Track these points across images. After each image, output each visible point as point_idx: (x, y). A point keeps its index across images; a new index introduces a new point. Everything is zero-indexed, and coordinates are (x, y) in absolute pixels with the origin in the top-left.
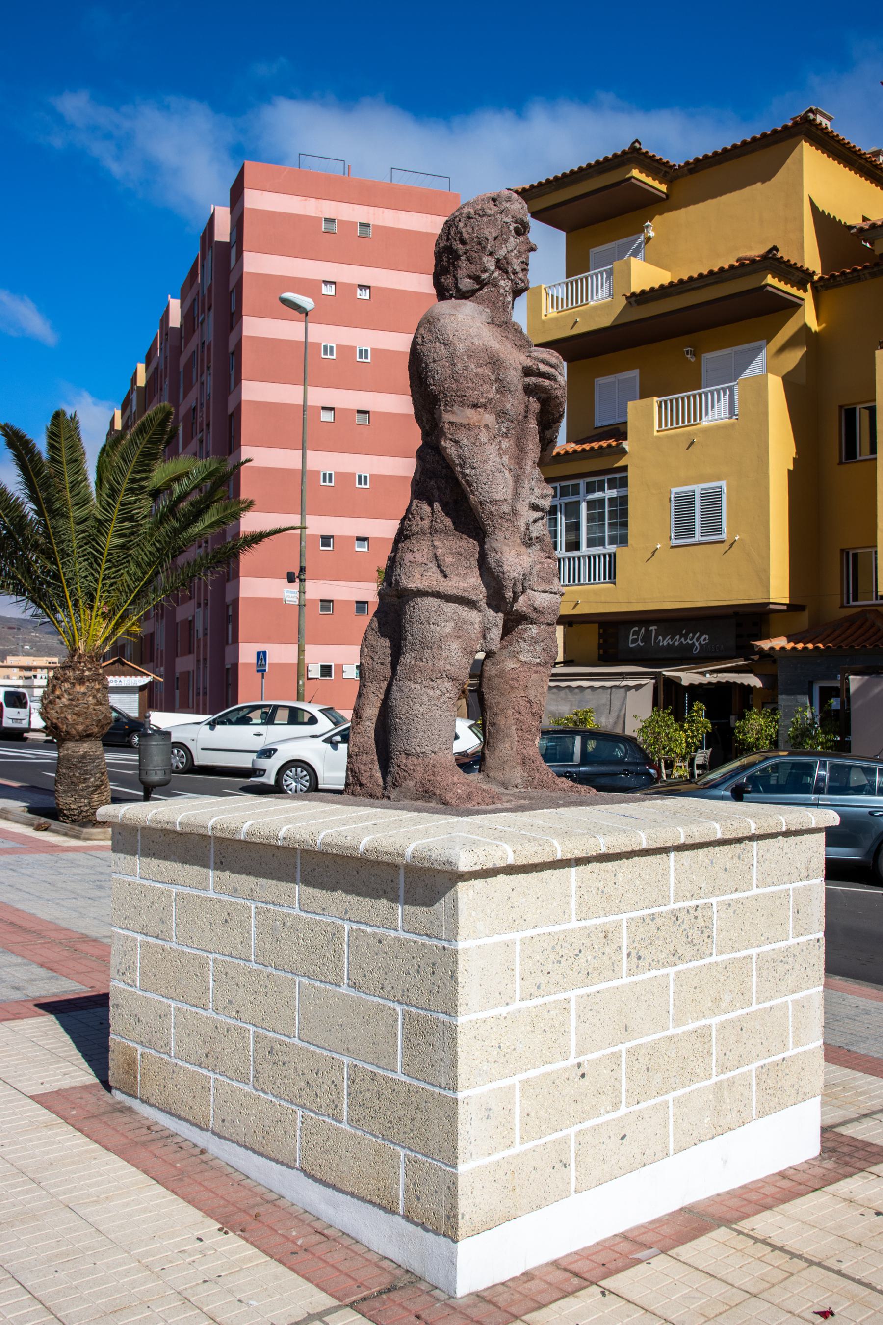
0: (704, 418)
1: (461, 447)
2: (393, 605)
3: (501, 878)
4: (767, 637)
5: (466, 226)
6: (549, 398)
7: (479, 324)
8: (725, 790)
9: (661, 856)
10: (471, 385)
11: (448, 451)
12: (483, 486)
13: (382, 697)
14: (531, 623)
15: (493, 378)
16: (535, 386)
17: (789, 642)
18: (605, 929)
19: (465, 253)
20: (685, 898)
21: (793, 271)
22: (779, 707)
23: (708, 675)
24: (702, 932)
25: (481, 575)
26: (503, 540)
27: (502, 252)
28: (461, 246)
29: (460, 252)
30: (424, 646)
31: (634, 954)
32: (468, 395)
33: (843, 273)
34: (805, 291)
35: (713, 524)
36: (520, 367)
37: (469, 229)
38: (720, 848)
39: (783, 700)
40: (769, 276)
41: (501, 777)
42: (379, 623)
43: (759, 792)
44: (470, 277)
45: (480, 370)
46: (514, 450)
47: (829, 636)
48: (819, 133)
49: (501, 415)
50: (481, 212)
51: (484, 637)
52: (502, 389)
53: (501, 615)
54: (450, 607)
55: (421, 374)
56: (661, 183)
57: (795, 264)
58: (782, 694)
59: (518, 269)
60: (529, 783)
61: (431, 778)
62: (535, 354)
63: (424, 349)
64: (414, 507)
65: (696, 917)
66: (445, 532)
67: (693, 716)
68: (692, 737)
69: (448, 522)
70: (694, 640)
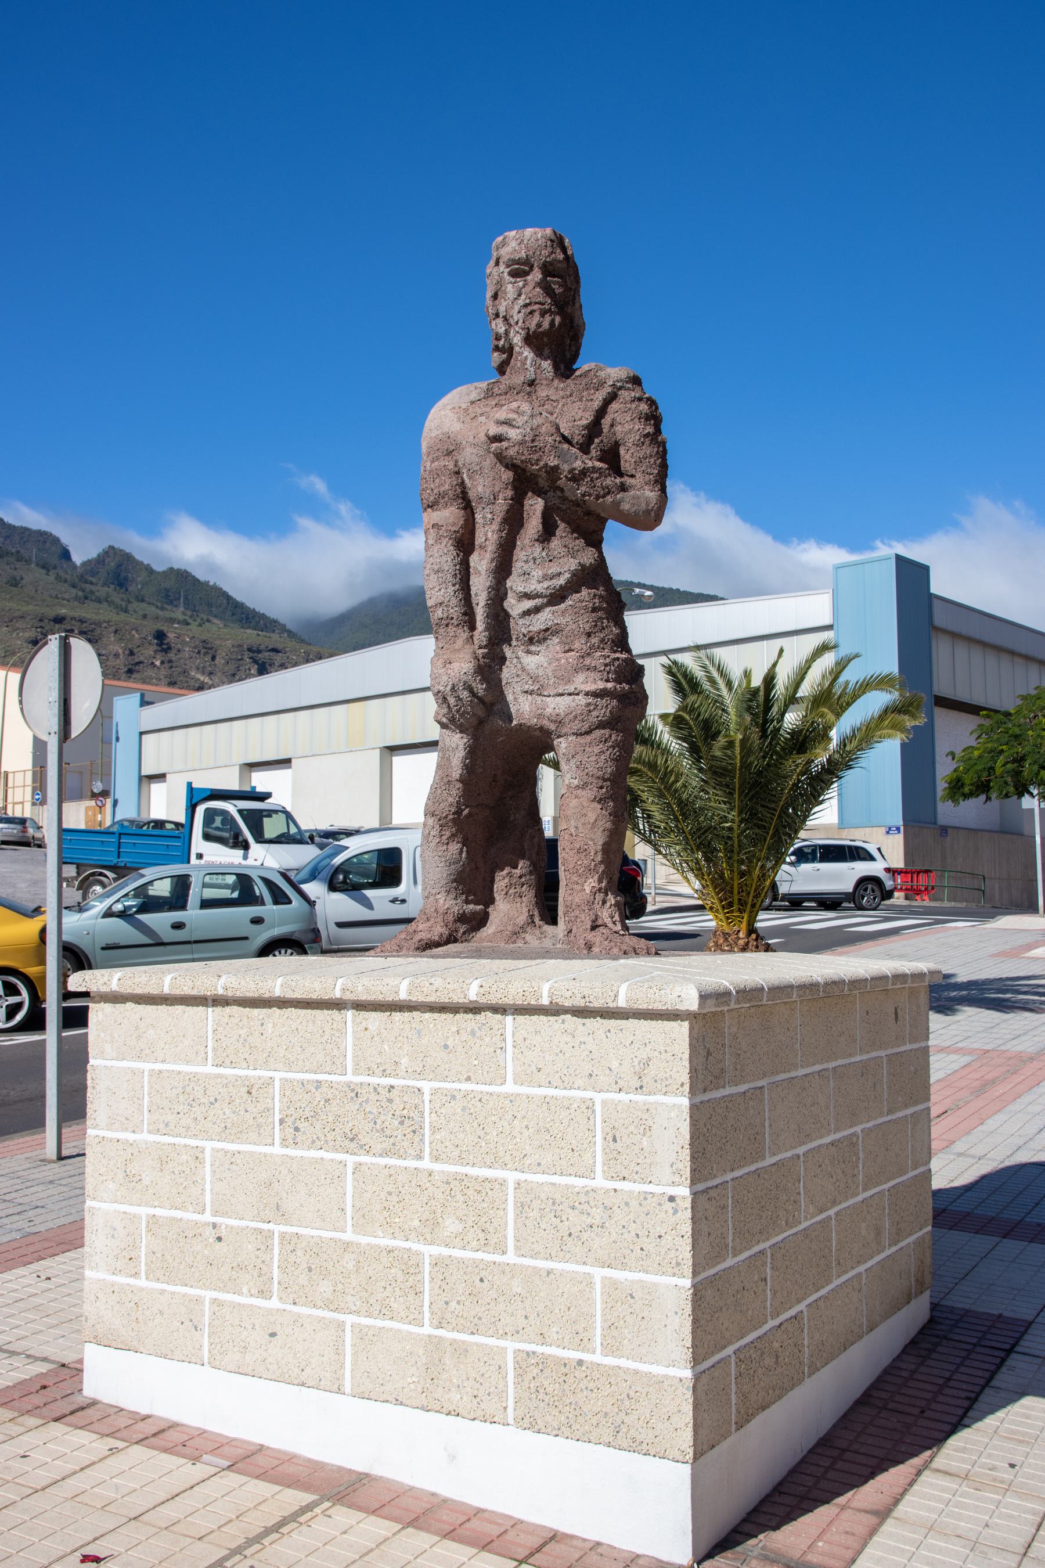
3: (130, 1005)
9: (330, 1012)
18: (247, 1083)
20: (370, 1072)
24: (402, 1123)
31: (289, 1121)
38: (436, 1015)
65: (390, 1101)
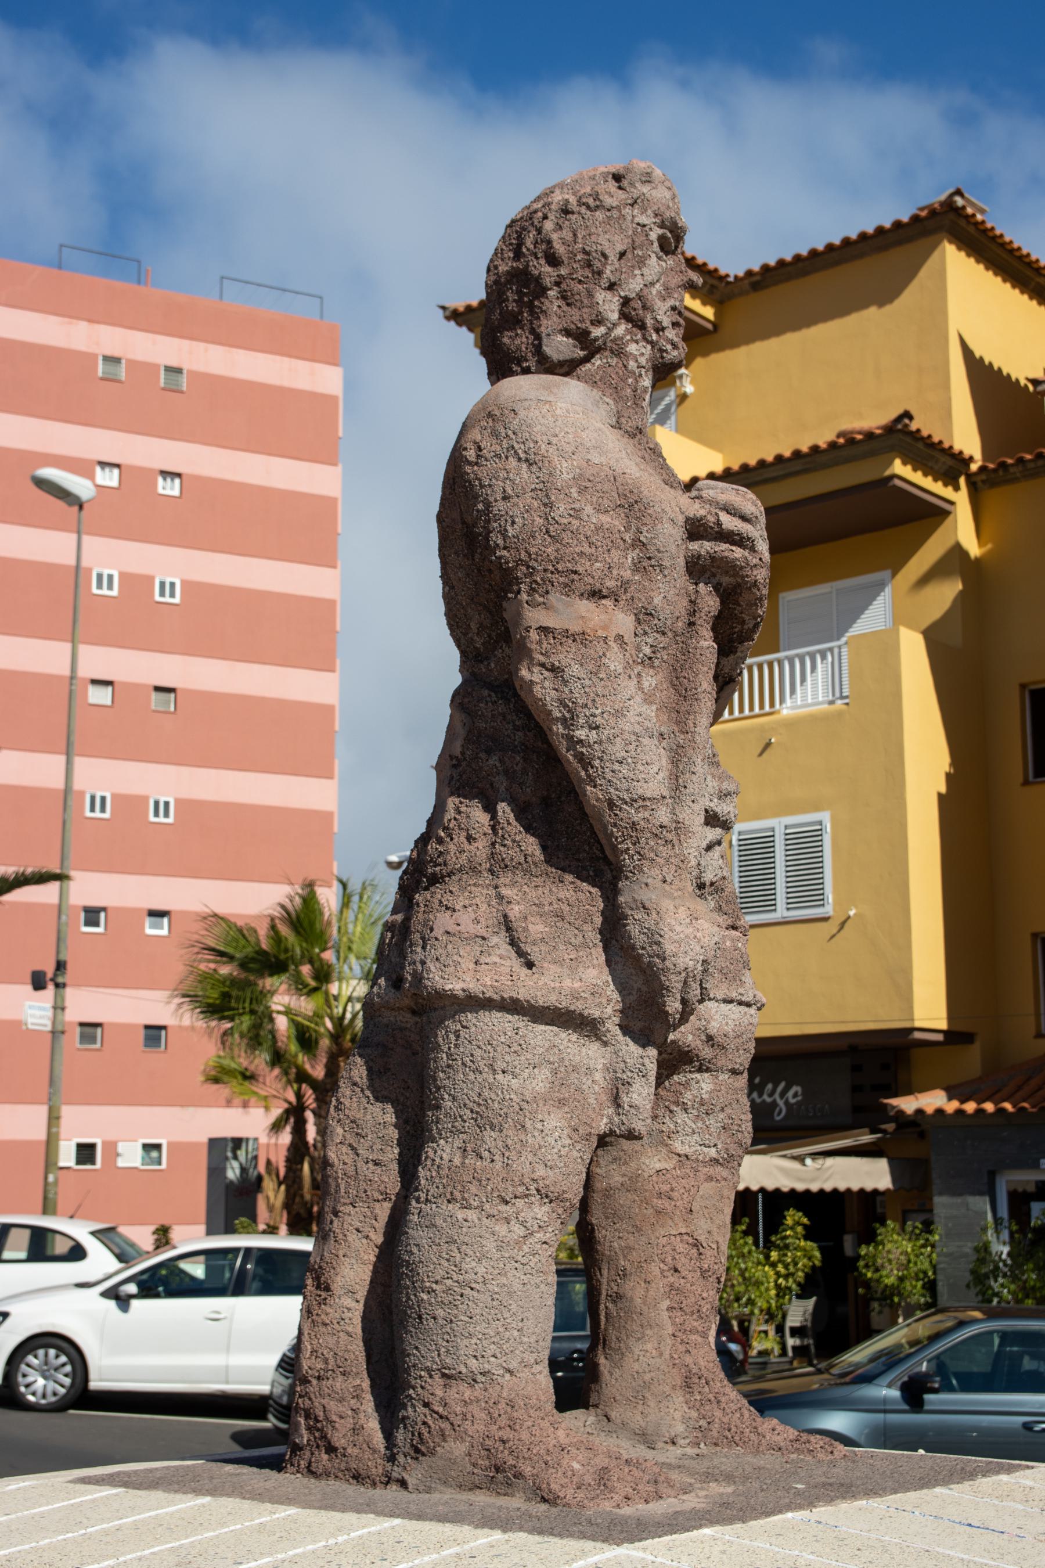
0: (788, 702)
1: (565, 682)
2: (401, 1029)
4: (908, 1090)
5: (559, 227)
6: (739, 585)
7: (599, 425)
8: (889, 1386)
10: (587, 549)
11: (537, 689)
12: (617, 766)
13: (379, 1239)
14: (700, 1070)
15: (627, 537)
16: (713, 558)
17: (950, 1098)
19: (558, 284)
21: (936, 454)
22: (936, 1219)
23: (808, 1161)
25: (608, 962)
26: (659, 884)
27: (633, 286)
28: (548, 269)
29: (547, 281)
30: (483, 1121)
32: (580, 569)
33: (1021, 461)
34: (957, 488)
35: (807, 887)
36: (681, 519)
37: (567, 234)
39: (942, 1204)
40: (898, 462)
41: (637, 1420)
42: (370, 1070)
43: (951, 1389)
44: (567, 333)
45: (605, 519)
46: (666, 694)
47: (1019, 1088)
48: (971, 229)
49: (644, 616)
50: (591, 201)
51: (616, 1101)
52: (645, 563)
53: (653, 1052)
54: (542, 1035)
55: (475, 525)
56: (704, 303)
57: (941, 442)
58: (941, 1194)
59: (666, 322)
60: (701, 1433)
61: (506, 1434)
62: (711, 492)
63: (482, 472)
64: (450, 813)
66: (525, 867)
67: (786, 1237)
68: (786, 1277)
69: (531, 845)
70: (777, 1096)
